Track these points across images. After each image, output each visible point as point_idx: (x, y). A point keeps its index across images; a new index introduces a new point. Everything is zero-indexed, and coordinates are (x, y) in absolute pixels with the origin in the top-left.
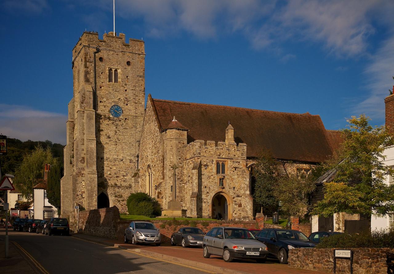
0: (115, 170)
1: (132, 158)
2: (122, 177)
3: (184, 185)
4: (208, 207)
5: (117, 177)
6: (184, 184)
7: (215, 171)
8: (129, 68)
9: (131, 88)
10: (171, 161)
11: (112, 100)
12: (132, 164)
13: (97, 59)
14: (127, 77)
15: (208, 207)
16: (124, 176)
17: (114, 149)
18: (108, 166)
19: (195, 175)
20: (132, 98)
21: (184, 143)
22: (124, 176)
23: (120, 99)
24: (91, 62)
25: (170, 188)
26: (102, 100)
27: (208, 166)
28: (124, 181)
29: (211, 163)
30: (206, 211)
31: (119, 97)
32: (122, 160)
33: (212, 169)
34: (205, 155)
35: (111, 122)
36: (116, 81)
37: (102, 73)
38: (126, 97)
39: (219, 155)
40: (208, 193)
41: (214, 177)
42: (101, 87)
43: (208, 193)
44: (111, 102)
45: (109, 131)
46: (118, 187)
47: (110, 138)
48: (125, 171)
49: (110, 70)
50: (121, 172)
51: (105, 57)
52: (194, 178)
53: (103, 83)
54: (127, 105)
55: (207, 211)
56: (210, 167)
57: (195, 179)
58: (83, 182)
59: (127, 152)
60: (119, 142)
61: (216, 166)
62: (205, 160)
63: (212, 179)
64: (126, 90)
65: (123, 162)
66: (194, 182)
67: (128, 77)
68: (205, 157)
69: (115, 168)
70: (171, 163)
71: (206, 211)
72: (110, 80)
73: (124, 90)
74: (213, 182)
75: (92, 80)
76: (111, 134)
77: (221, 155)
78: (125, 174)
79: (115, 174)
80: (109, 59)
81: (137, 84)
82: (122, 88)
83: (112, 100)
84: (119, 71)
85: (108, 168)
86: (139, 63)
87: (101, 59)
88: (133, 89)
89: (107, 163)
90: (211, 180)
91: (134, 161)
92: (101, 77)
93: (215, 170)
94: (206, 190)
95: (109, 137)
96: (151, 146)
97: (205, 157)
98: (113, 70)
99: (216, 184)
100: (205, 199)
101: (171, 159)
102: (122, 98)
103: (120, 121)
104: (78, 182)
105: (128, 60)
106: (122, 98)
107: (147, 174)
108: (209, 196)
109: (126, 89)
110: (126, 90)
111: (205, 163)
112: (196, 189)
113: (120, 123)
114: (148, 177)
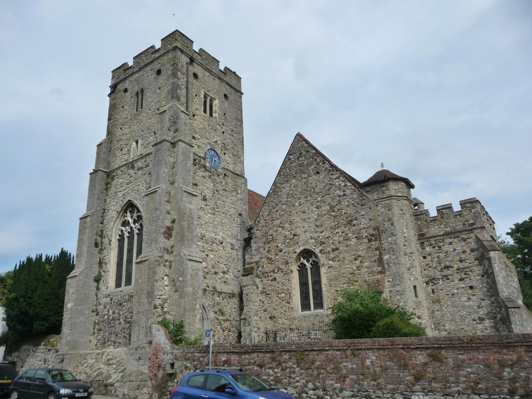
0: (212, 259)
1: (234, 241)
2: (222, 274)
5: (216, 273)
10: (405, 237)
12: (234, 252)
13: (191, 73)
14: (224, 114)
16: (224, 273)
17: (212, 221)
18: (203, 249)
20: (230, 147)
22: (224, 273)
23: (216, 142)
25: (413, 291)
28: (225, 282)
31: (215, 140)
32: (222, 243)
35: (207, 174)
37: (196, 96)
38: (224, 142)
42: (194, 116)
45: (204, 188)
46: (219, 292)
47: (206, 200)
48: (225, 263)
50: (220, 265)
52: (497, 268)
53: (196, 109)
54: (225, 154)
57: (501, 269)
58: (166, 278)
59: (227, 229)
60: (217, 210)
65: (223, 247)
66: (498, 276)
67: (226, 115)
69: (212, 256)
70: (406, 241)
72: (205, 111)
73: (222, 132)
76: (208, 194)
78: (225, 269)
79: (213, 267)
81: (235, 129)
83: (208, 140)
84: (216, 102)
85: (204, 254)
87: (195, 76)
88: (231, 133)
89: (202, 245)
91: (236, 247)
92: (195, 100)
95: (205, 199)
98: (209, 98)
101: (404, 233)
103: (218, 175)
104: (157, 277)
107: (295, 268)
110: (223, 133)
112: (506, 291)
113: (218, 180)
114: (295, 276)
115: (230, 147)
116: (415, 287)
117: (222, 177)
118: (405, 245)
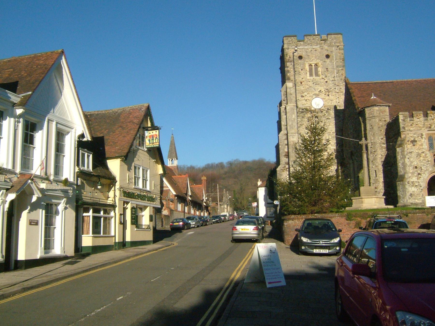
3: (389, 168)
4: (420, 192)
6: (389, 167)
7: (426, 147)
8: (328, 61)
9: (331, 79)
11: (313, 93)
15: (420, 192)
19: (400, 154)
21: (385, 121)
23: (320, 91)
24: (291, 62)
26: (303, 95)
27: (416, 141)
29: (420, 137)
30: (419, 197)
31: (319, 90)
33: (422, 145)
34: (411, 129)
36: (317, 75)
38: (327, 88)
39: (430, 127)
40: (419, 174)
41: (426, 155)
42: (301, 83)
43: (419, 174)
44: (312, 95)
49: (311, 65)
51: (304, 55)
52: (399, 158)
54: (328, 95)
55: (420, 196)
56: (419, 143)
61: (427, 141)
62: (411, 135)
63: (424, 157)
64: (327, 82)
68: (411, 131)
71: (419, 197)
72: (311, 75)
73: (324, 82)
74: (425, 160)
75: (292, 78)
77: (433, 127)
80: (308, 56)
82: (322, 80)
86: (337, 54)
87: (300, 57)
90: (422, 158)
93: (426, 146)
94: (417, 171)
96: (352, 131)
97: (411, 131)
98: (313, 65)
99: (430, 162)
100: (416, 182)
102: (323, 90)
105: (327, 53)
106: (323, 90)
108: (422, 178)
109: (326, 80)
111: (412, 139)
114: (351, 165)
115: (333, 89)
116: (376, 171)
117: (325, 111)
118: (371, 148)
